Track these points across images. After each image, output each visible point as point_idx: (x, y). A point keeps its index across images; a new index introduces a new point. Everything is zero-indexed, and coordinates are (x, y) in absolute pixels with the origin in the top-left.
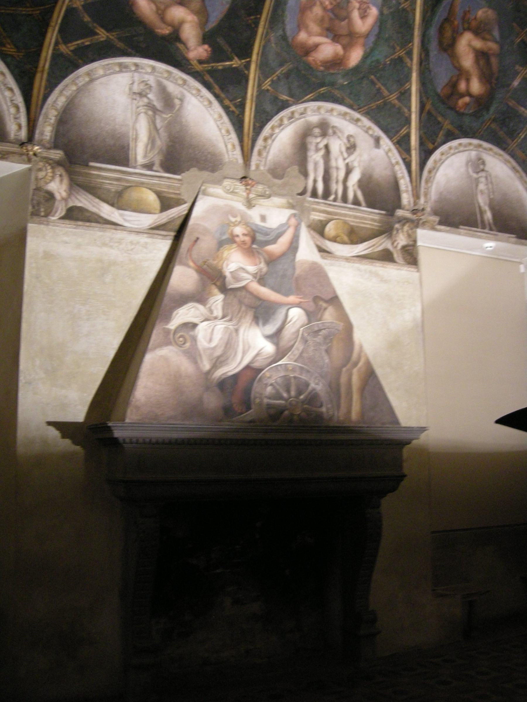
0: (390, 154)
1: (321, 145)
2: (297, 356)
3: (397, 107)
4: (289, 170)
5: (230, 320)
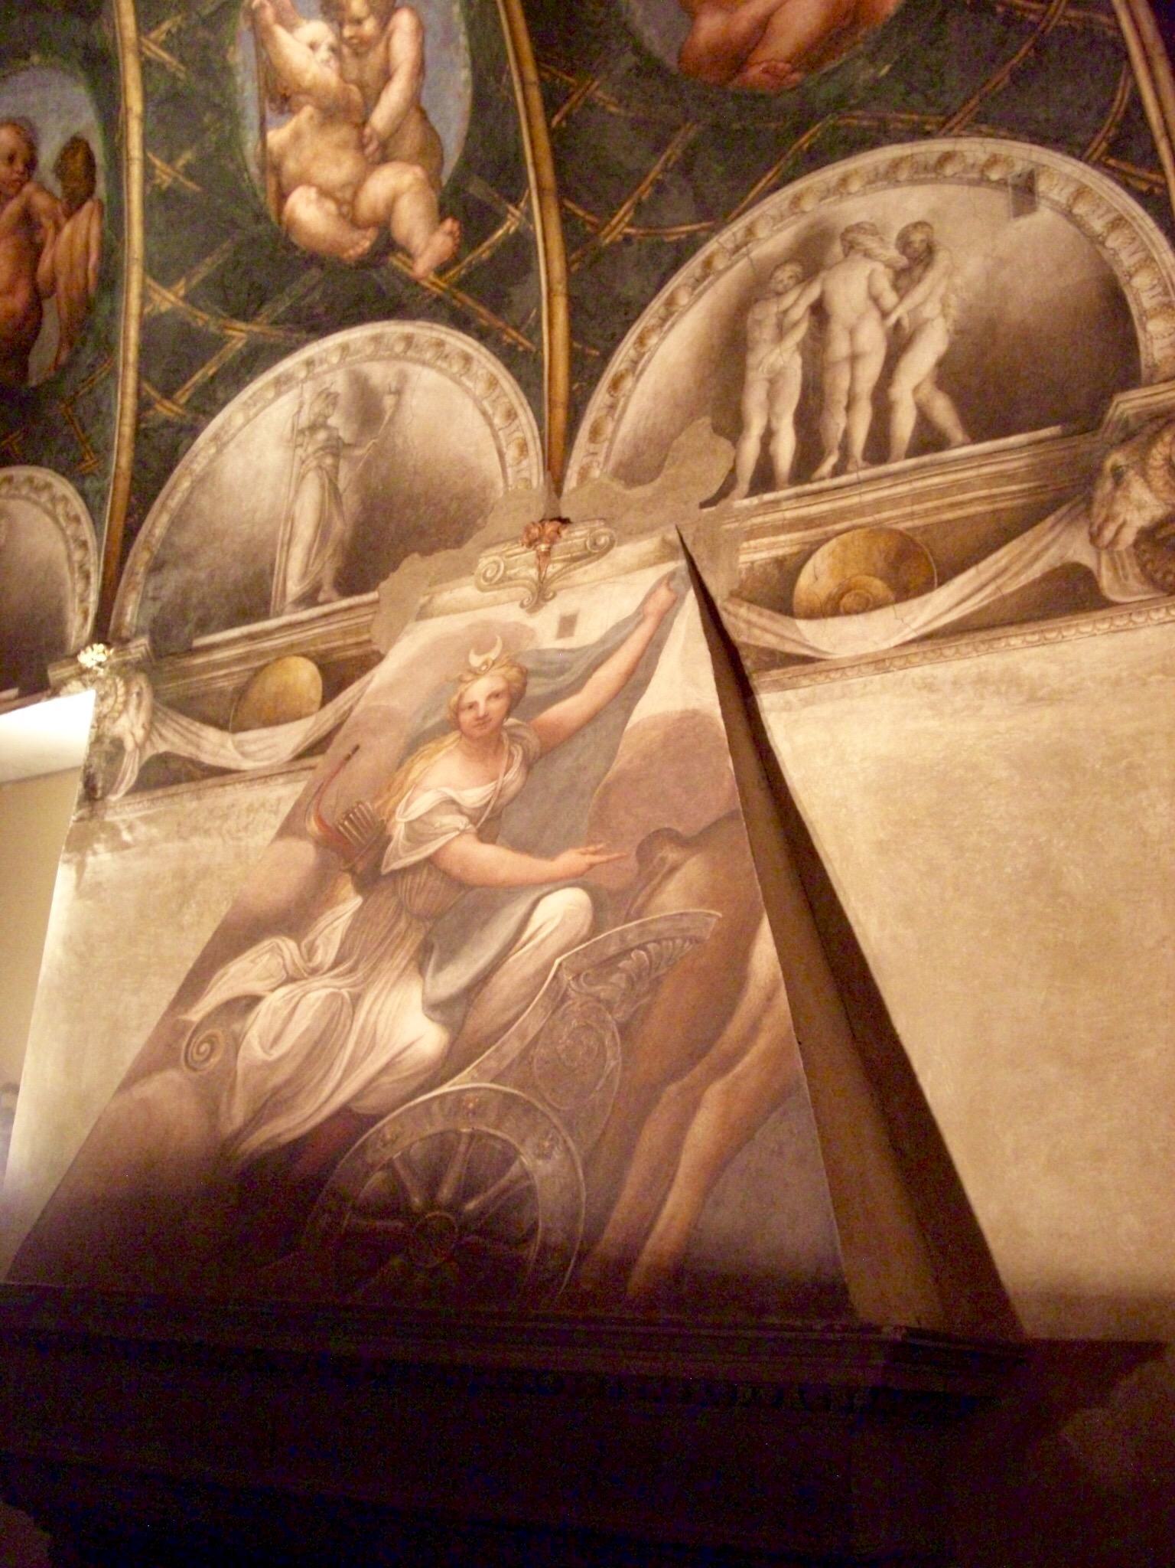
0: (1080, 209)
1: (800, 311)
2: (506, 1062)
3: (1079, 27)
4: (682, 438)
5: (352, 970)
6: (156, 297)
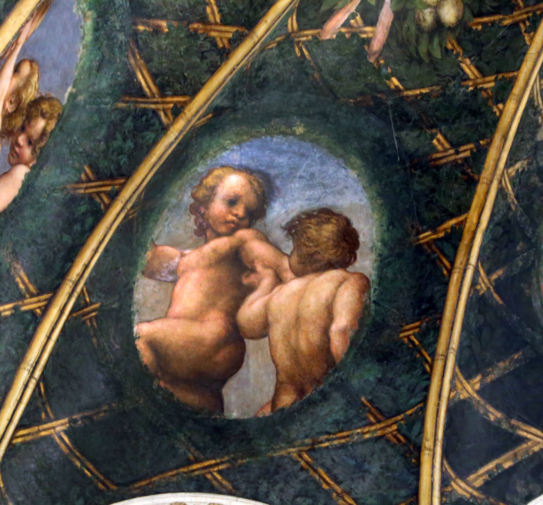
6: (459, 386)
